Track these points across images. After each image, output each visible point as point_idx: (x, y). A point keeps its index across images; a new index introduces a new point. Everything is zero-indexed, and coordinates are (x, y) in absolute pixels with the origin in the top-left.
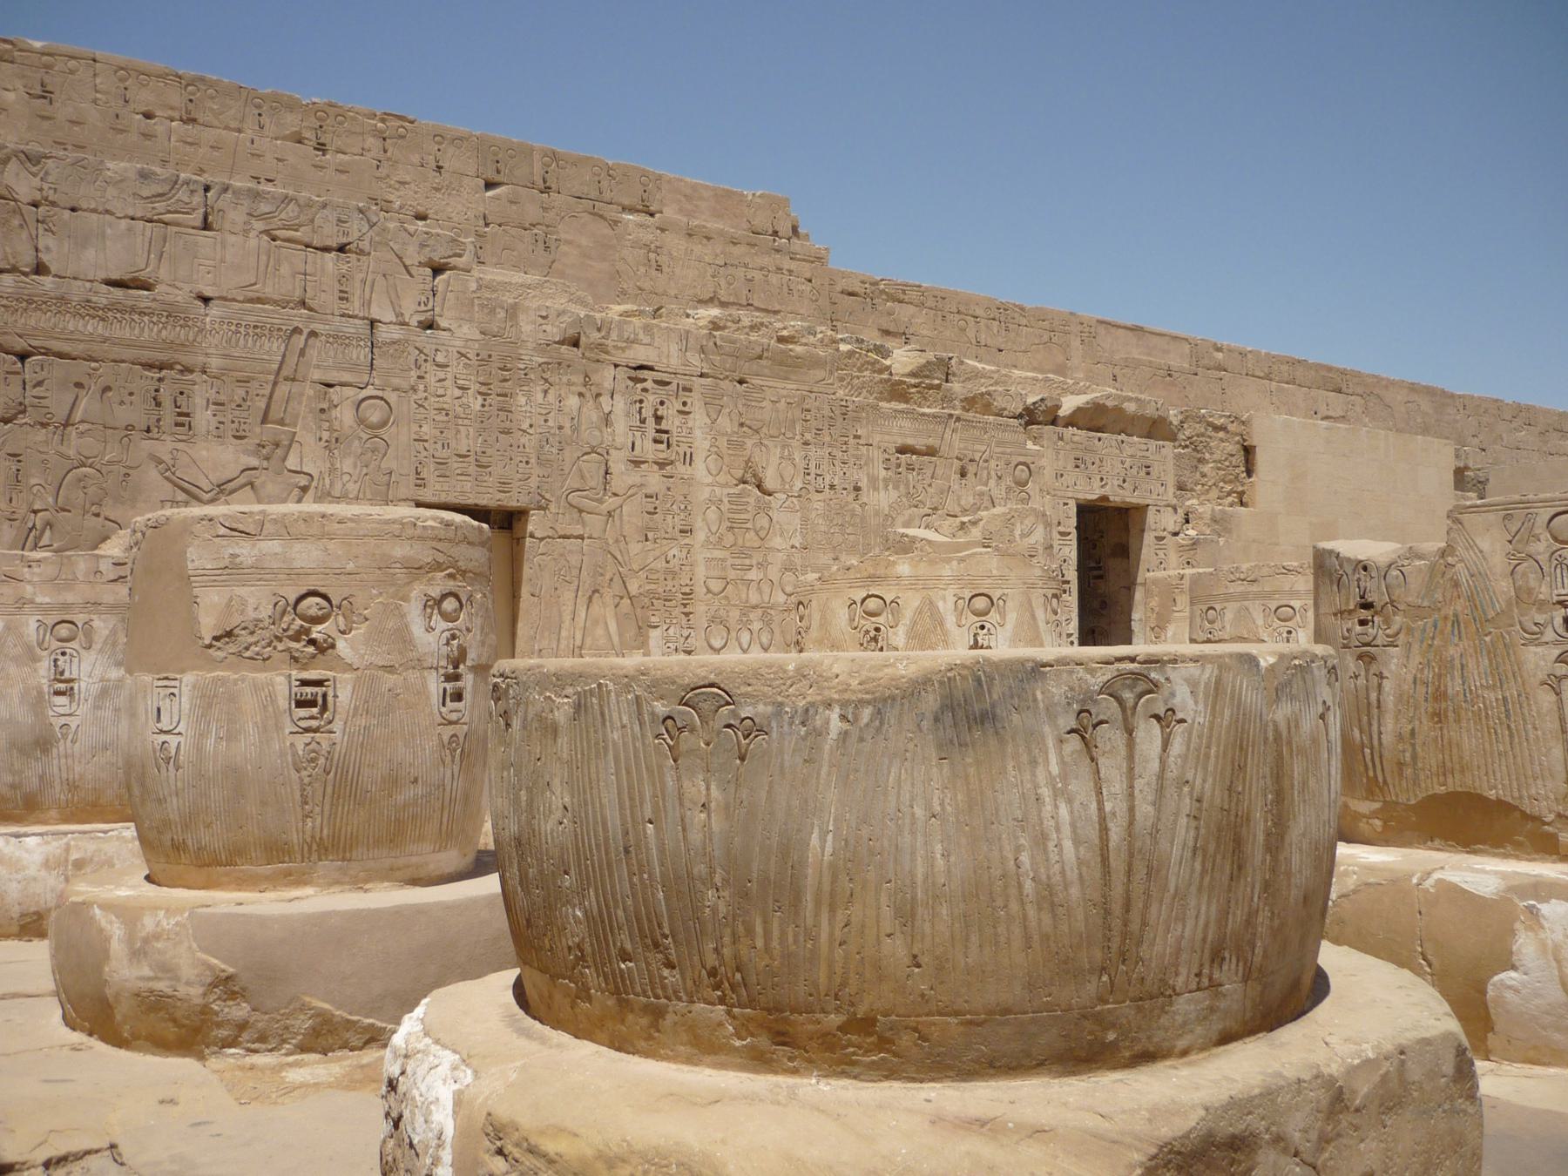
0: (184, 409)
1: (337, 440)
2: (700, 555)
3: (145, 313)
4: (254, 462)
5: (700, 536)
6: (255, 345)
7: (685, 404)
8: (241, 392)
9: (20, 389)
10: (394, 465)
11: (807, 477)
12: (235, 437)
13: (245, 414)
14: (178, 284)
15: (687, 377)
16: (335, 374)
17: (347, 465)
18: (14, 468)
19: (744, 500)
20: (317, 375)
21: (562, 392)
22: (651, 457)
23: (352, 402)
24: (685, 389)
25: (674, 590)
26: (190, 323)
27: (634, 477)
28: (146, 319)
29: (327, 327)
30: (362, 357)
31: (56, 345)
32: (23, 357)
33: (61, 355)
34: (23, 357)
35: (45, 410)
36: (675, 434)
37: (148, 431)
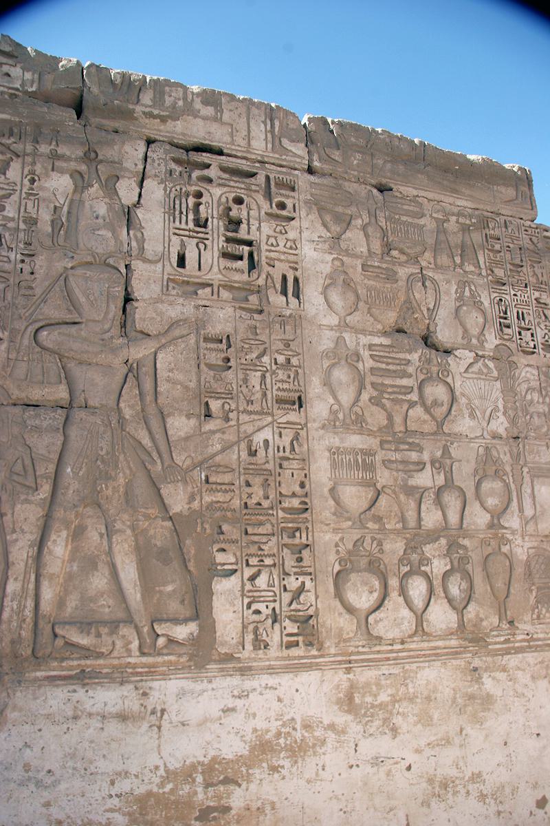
2: (321, 445)
5: (319, 408)
7: (282, 206)
11: (506, 330)
15: (284, 170)
19: (401, 356)
21: (38, 168)
22: (215, 276)
24: (281, 185)
25: (266, 504)
27: (179, 308)
36: (264, 247)
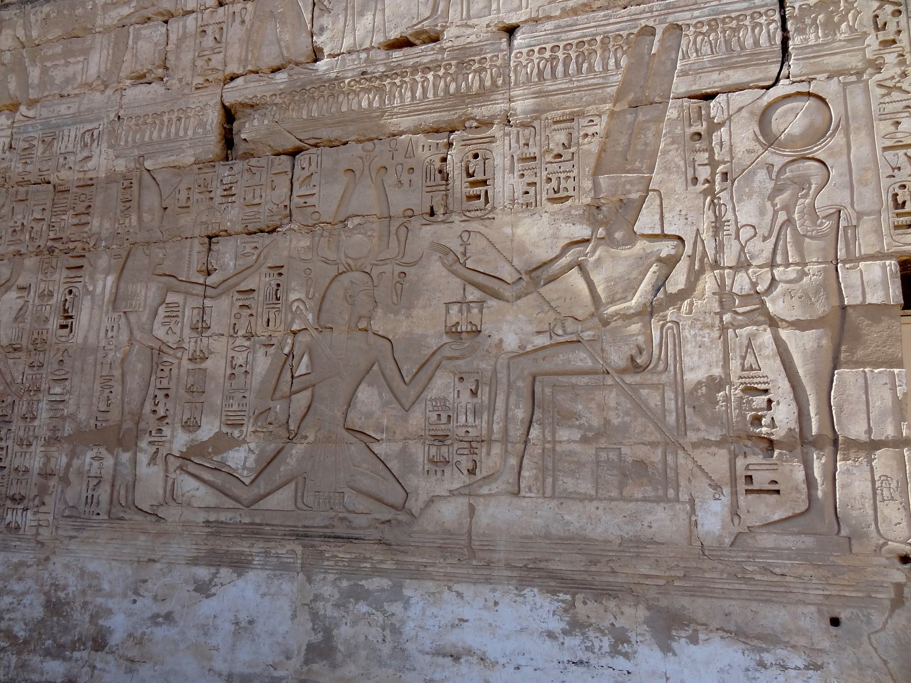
0: (479, 177)
1: (725, 175)
3: (429, 68)
4: (582, 231)
6: (579, 70)
8: (561, 137)
9: (286, 190)
10: (842, 197)
12: (549, 199)
13: (567, 166)
14: (470, 23)
16: (715, 76)
17: (747, 213)
18: (274, 283)
20: (680, 85)
23: (752, 113)
26: (487, 65)
28: (430, 76)
29: (696, 13)
30: (763, 40)
31: (325, 134)
32: (294, 153)
33: (332, 144)
34: (294, 153)
35: (312, 209)
37: (432, 214)
